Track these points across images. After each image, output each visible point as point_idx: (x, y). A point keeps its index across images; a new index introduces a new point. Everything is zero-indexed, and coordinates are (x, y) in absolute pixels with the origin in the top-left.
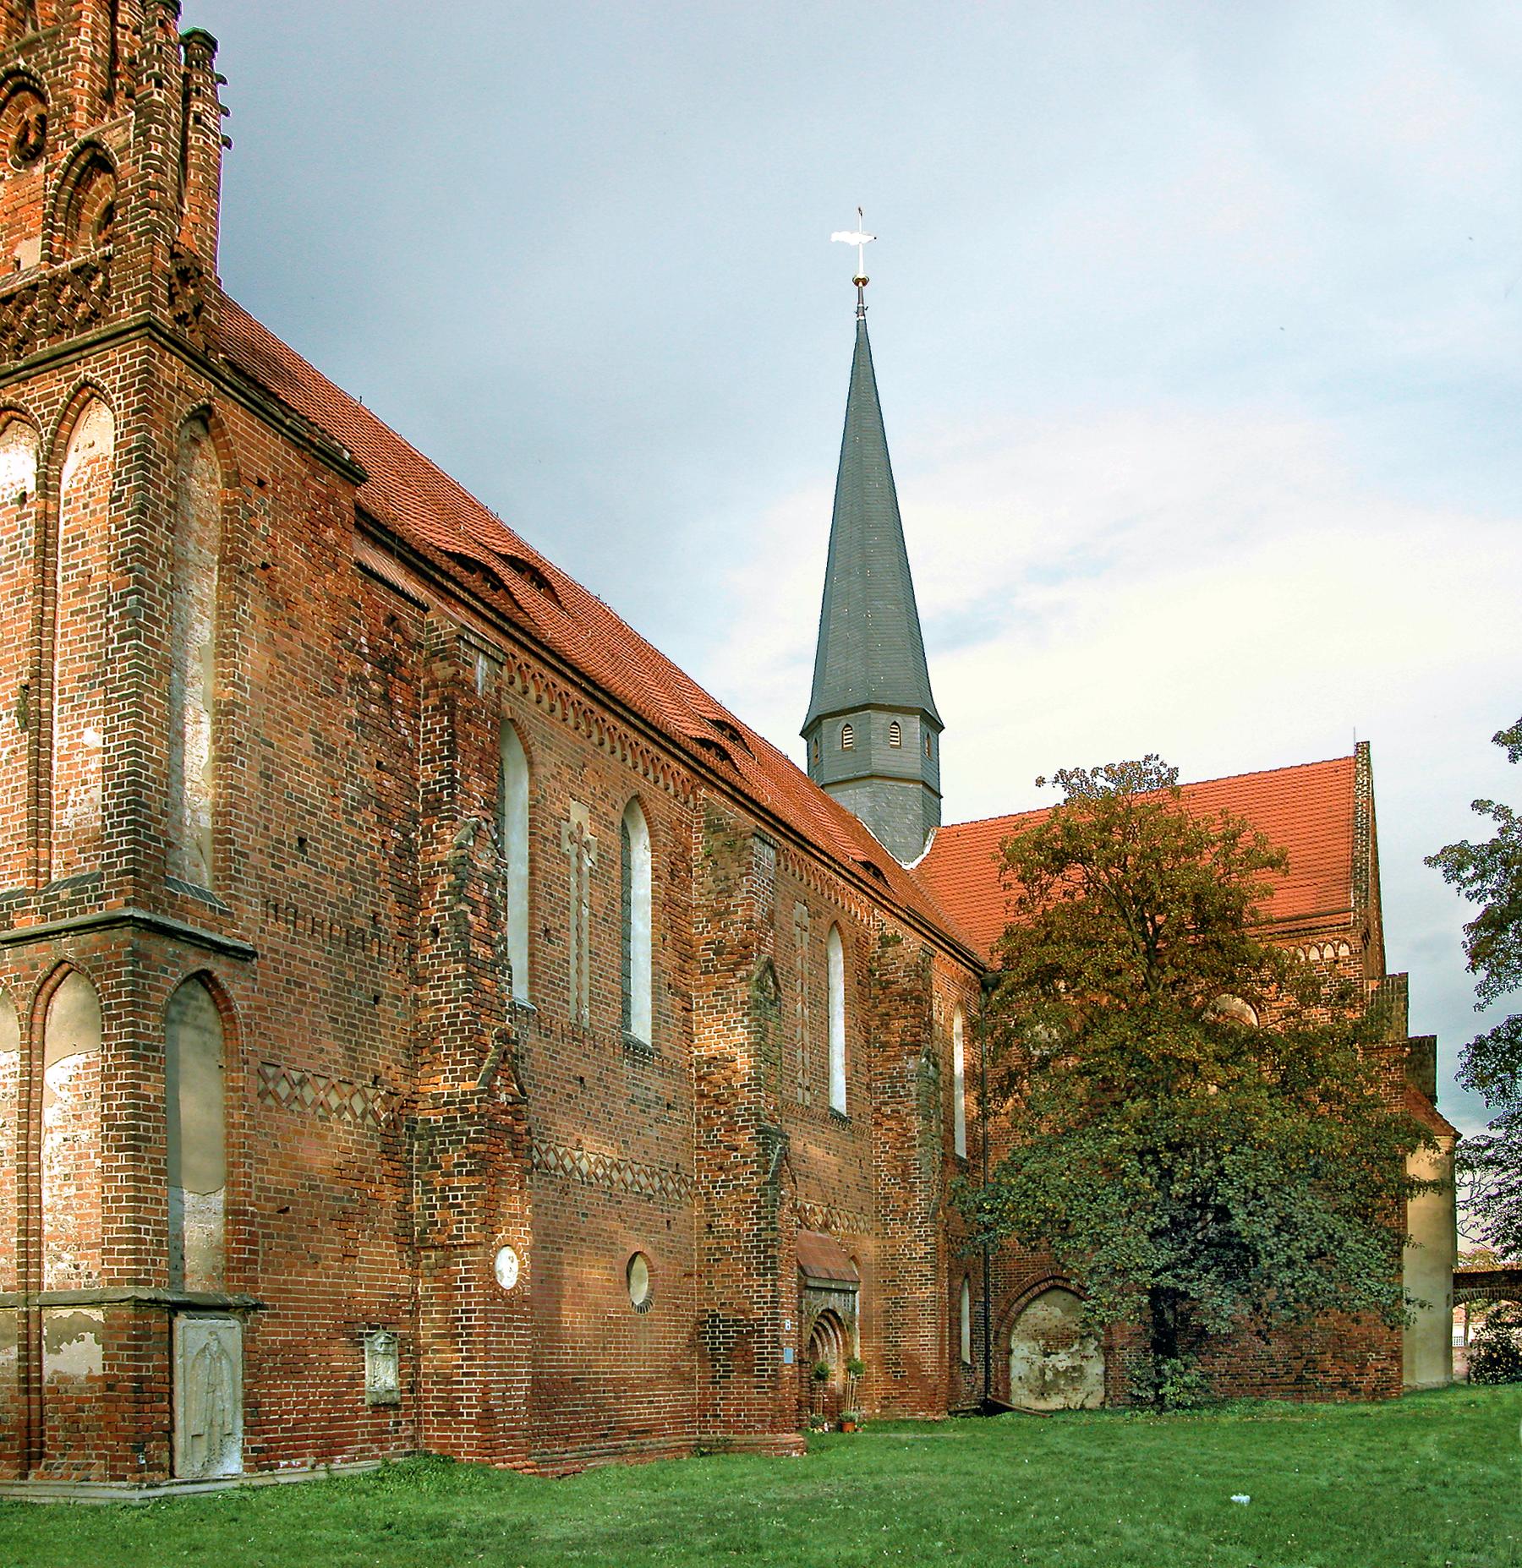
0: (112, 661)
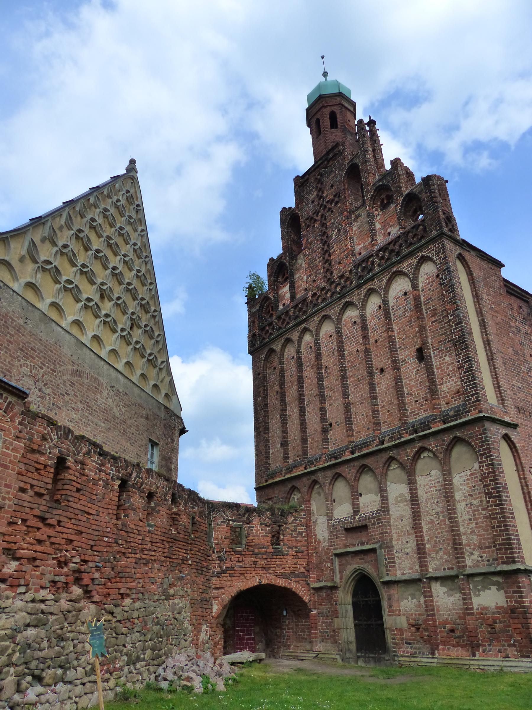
0: (454, 332)
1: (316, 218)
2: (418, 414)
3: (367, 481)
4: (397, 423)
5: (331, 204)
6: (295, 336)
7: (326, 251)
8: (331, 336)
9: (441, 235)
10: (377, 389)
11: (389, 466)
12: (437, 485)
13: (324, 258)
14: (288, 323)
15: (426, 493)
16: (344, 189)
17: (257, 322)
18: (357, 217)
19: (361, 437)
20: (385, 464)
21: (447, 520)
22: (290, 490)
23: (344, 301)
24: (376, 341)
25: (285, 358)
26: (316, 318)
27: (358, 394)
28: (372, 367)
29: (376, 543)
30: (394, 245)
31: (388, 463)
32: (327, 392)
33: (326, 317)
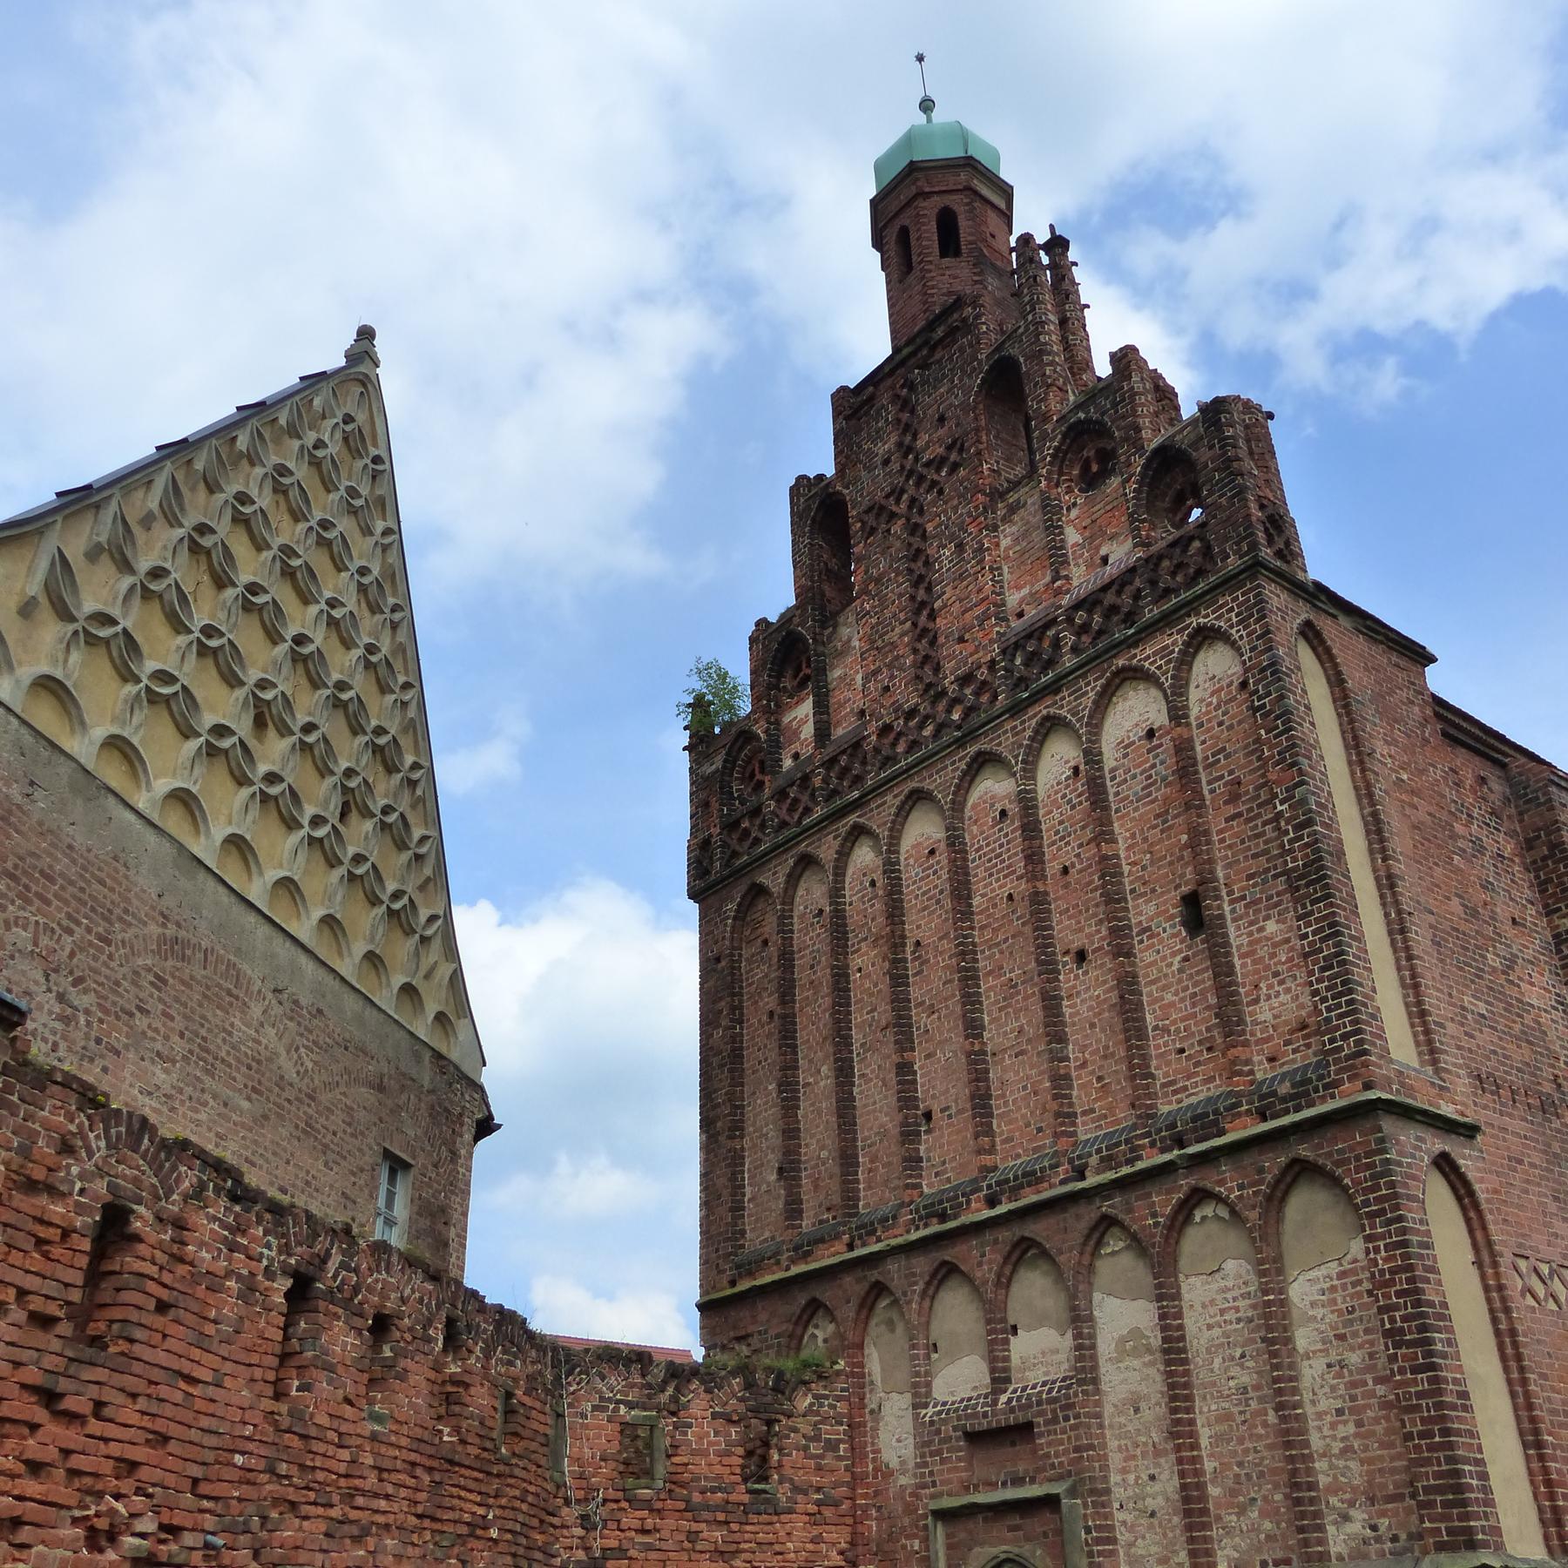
0: (1291, 851)
1: (894, 508)
2: (1185, 1088)
3: (1033, 1290)
4: (1125, 1116)
5: (938, 470)
6: (826, 849)
7: (923, 604)
8: (932, 852)
9: (1255, 567)
10: (1067, 1011)
11: (1099, 1244)
12: (1241, 1303)
13: (915, 625)
14: (807, 811)
15: (1210, 1327)
16: (977, 430)
17: (715, 805)
18: (1013, 509)
19: (1018, 1156)
20: (1088, 1237)
21: (1271, 1413)
22: (803, 1310)
23: (972, 750)
24: (1065, 871)
25: (796, 914)
26: (889, 798)
27: (1009, 1025)
28: (1052, 945)
29: (1060, 1478)
30: (1119, 593)
31: (1096, 1235)
32: (920, 1018)
33: (919, 797)
